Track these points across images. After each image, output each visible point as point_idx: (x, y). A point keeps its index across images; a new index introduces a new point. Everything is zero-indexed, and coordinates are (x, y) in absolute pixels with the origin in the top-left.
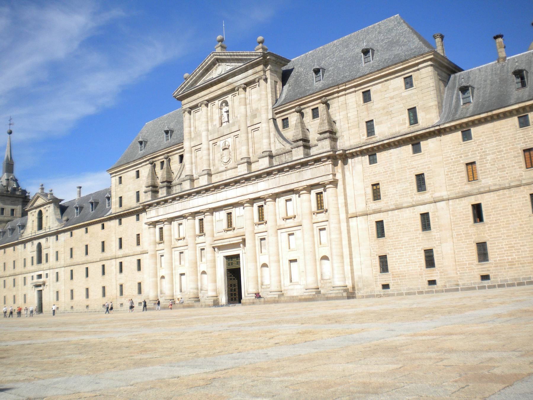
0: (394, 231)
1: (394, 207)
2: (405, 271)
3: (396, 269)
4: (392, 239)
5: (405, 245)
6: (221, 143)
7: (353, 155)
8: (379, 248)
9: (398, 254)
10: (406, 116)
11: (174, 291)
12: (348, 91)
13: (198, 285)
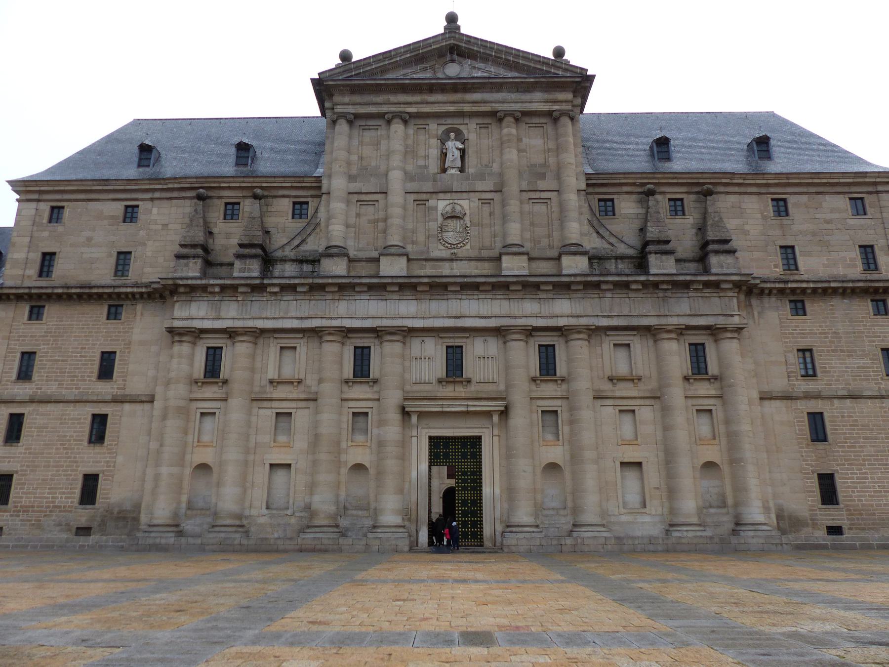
0: (845, 434)
1: (845, 393)
2: (872, 506)
3: (854, 501)
4: (844, 447)
5: (870, 460)
6: (442, 205)
7: (762, 292)
8: (816, 460)
9: (856, 474)
10: (855, 254)
11: (247, 504)
12: (742, 190)
13: (337, 496)
